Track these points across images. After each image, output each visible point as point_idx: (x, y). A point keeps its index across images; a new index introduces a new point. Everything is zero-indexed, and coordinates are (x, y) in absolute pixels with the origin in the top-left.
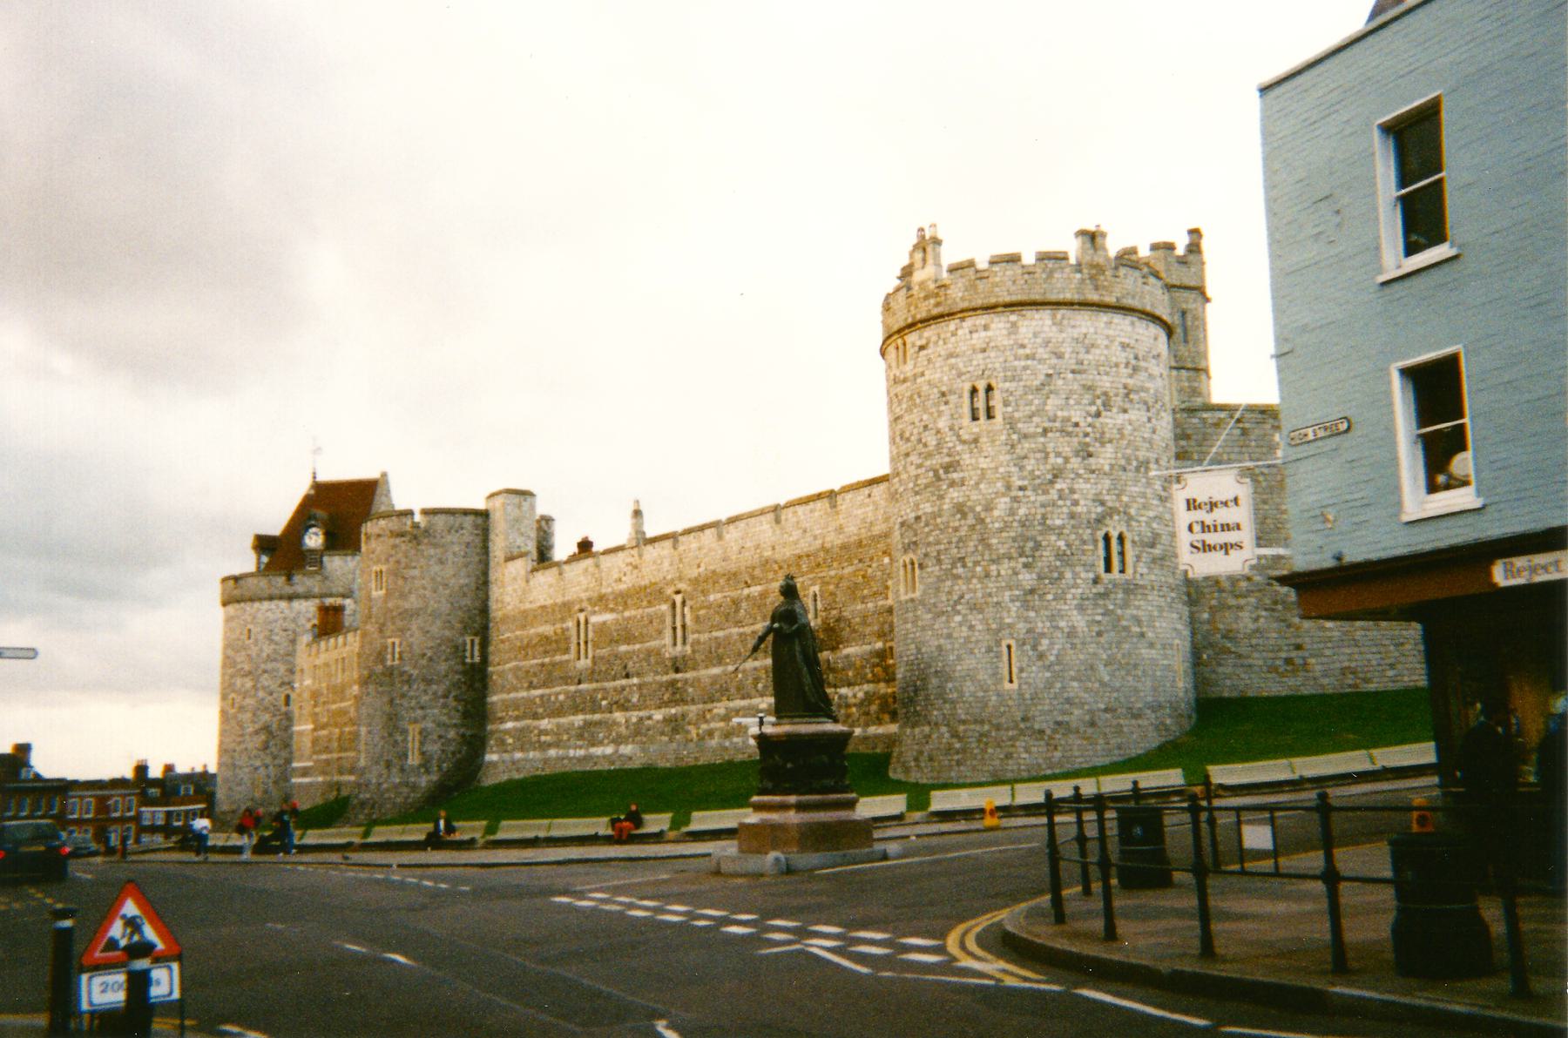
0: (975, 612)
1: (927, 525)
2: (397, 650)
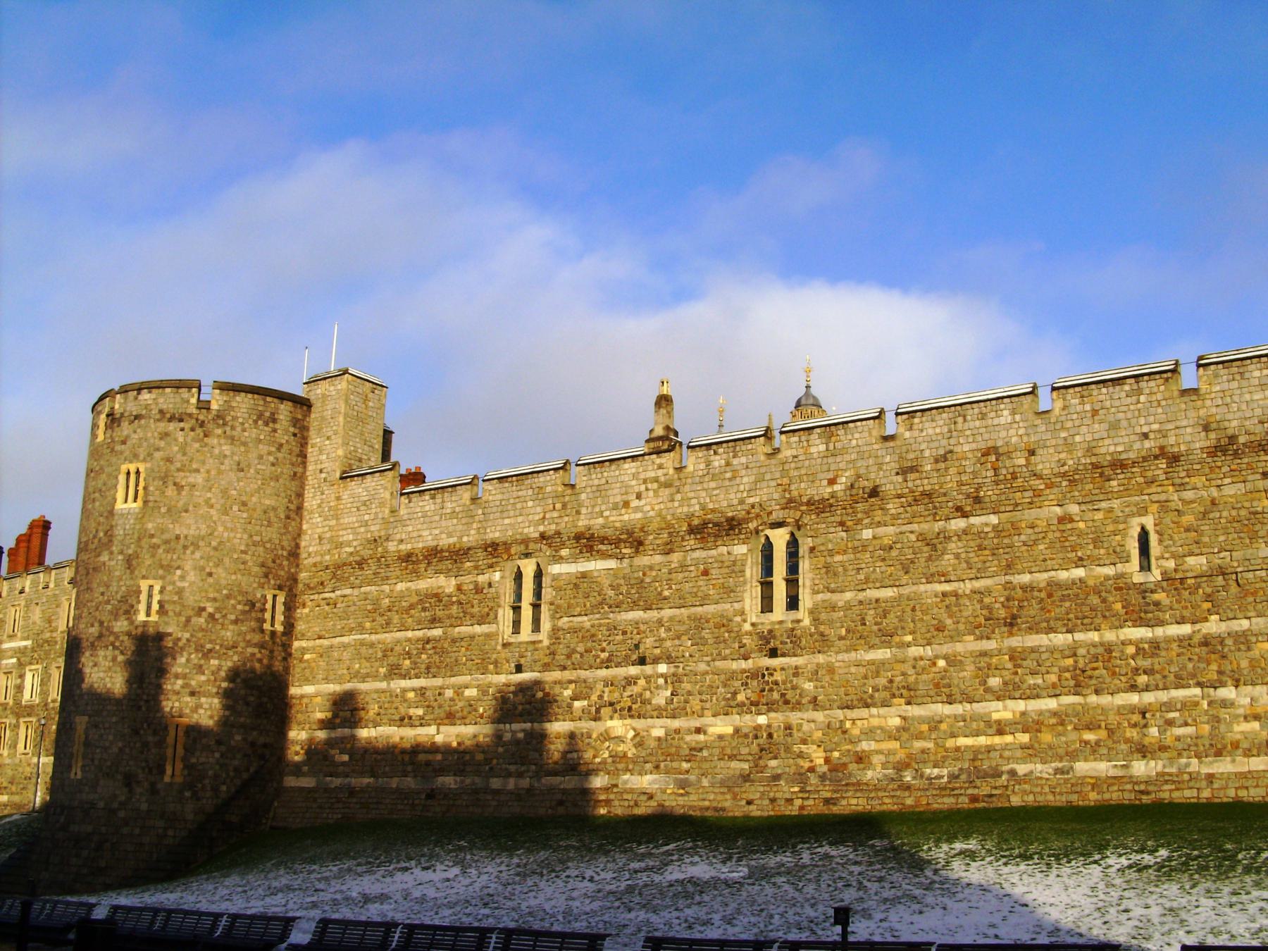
2: (156, 598)
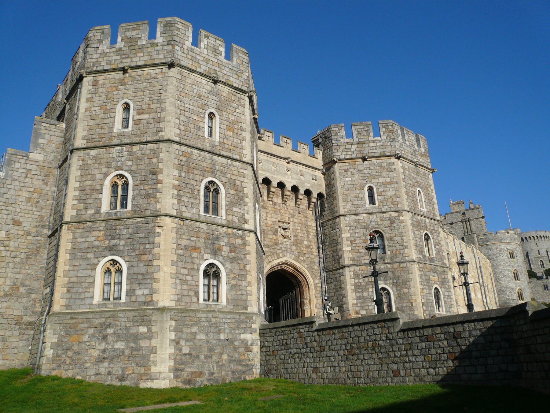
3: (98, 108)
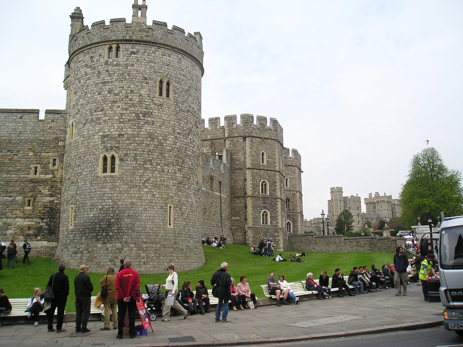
0: (156, 188)
1: (128, 139)
3: (254, 152)
